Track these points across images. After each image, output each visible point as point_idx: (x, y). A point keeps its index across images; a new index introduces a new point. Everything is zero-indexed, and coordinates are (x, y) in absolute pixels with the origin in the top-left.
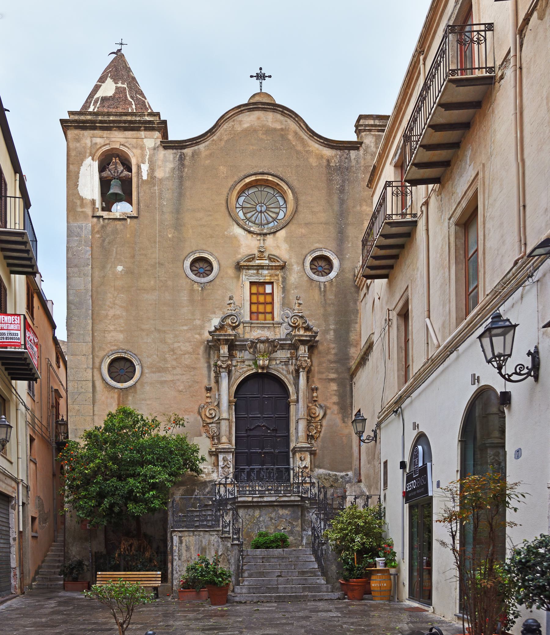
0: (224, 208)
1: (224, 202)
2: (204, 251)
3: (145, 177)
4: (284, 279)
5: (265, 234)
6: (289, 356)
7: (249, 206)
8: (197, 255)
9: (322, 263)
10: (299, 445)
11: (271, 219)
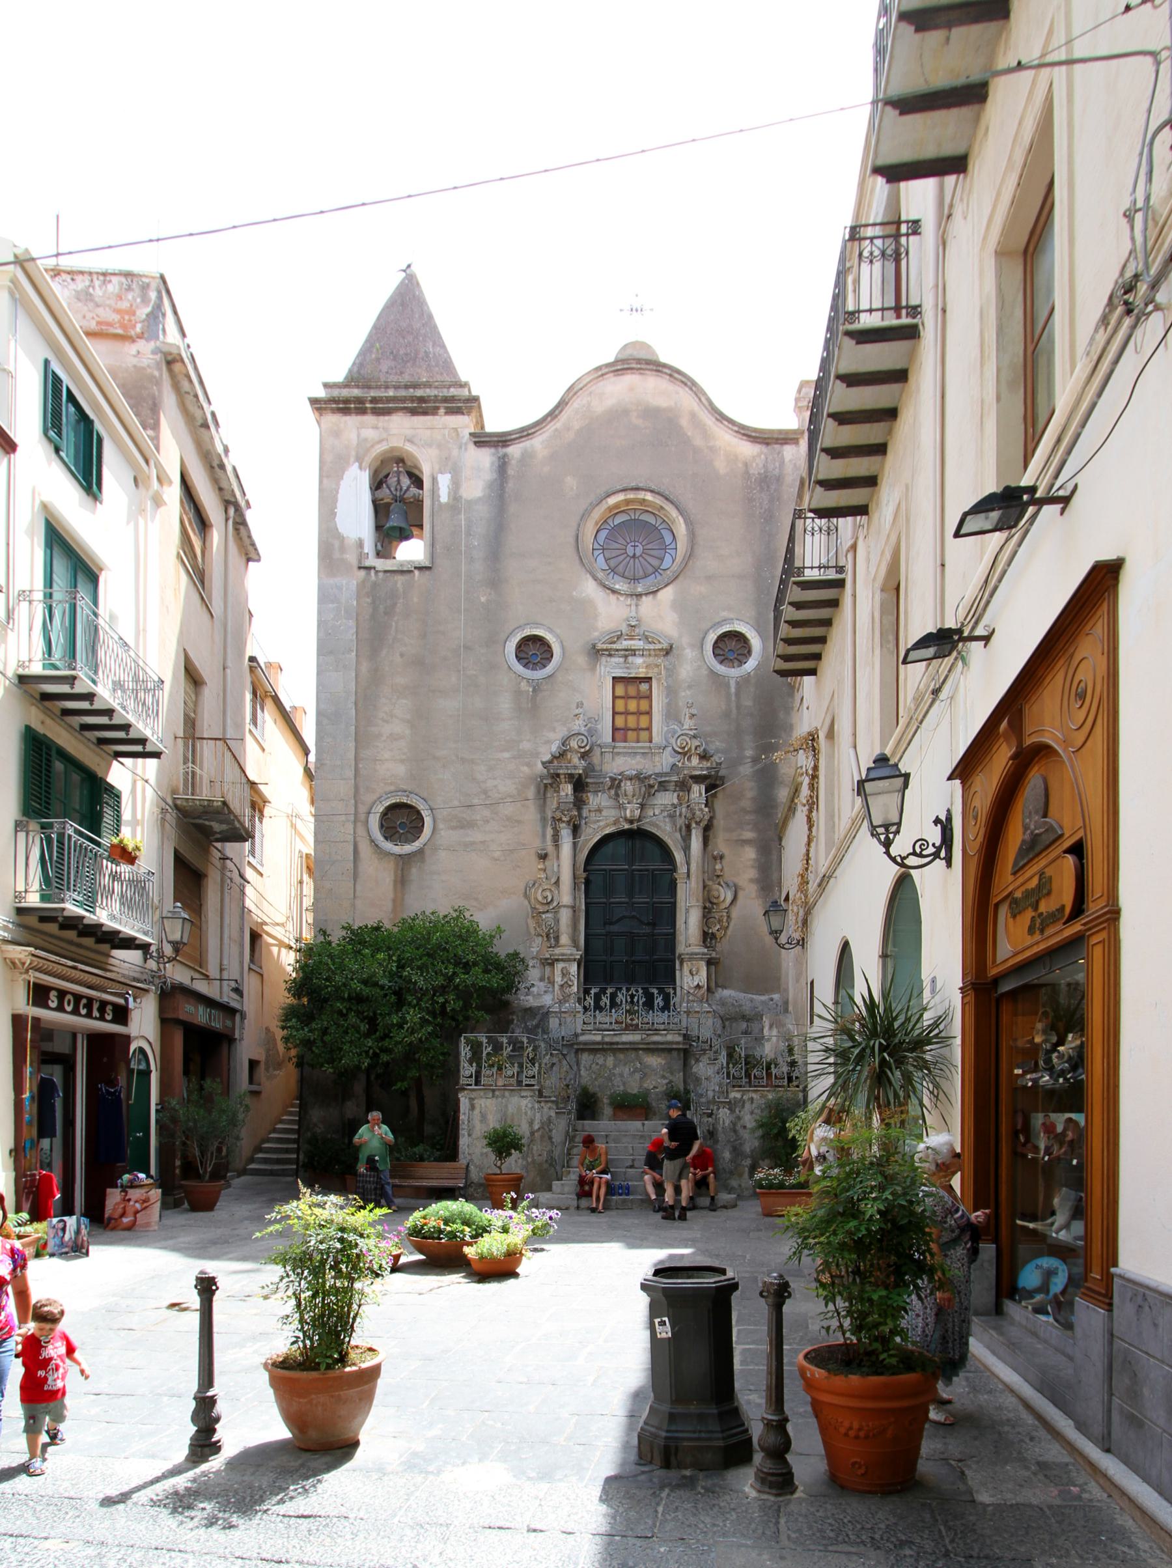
0: (570, 550)
1: (572, 540)
2: (538, 625)
3: (444, 497)
4: (671, 672)
5: (639, 596)
6: (676, 801)
8: (528, 632)
9: (732, 644)
10: (689, 950)
11: (651, 570)
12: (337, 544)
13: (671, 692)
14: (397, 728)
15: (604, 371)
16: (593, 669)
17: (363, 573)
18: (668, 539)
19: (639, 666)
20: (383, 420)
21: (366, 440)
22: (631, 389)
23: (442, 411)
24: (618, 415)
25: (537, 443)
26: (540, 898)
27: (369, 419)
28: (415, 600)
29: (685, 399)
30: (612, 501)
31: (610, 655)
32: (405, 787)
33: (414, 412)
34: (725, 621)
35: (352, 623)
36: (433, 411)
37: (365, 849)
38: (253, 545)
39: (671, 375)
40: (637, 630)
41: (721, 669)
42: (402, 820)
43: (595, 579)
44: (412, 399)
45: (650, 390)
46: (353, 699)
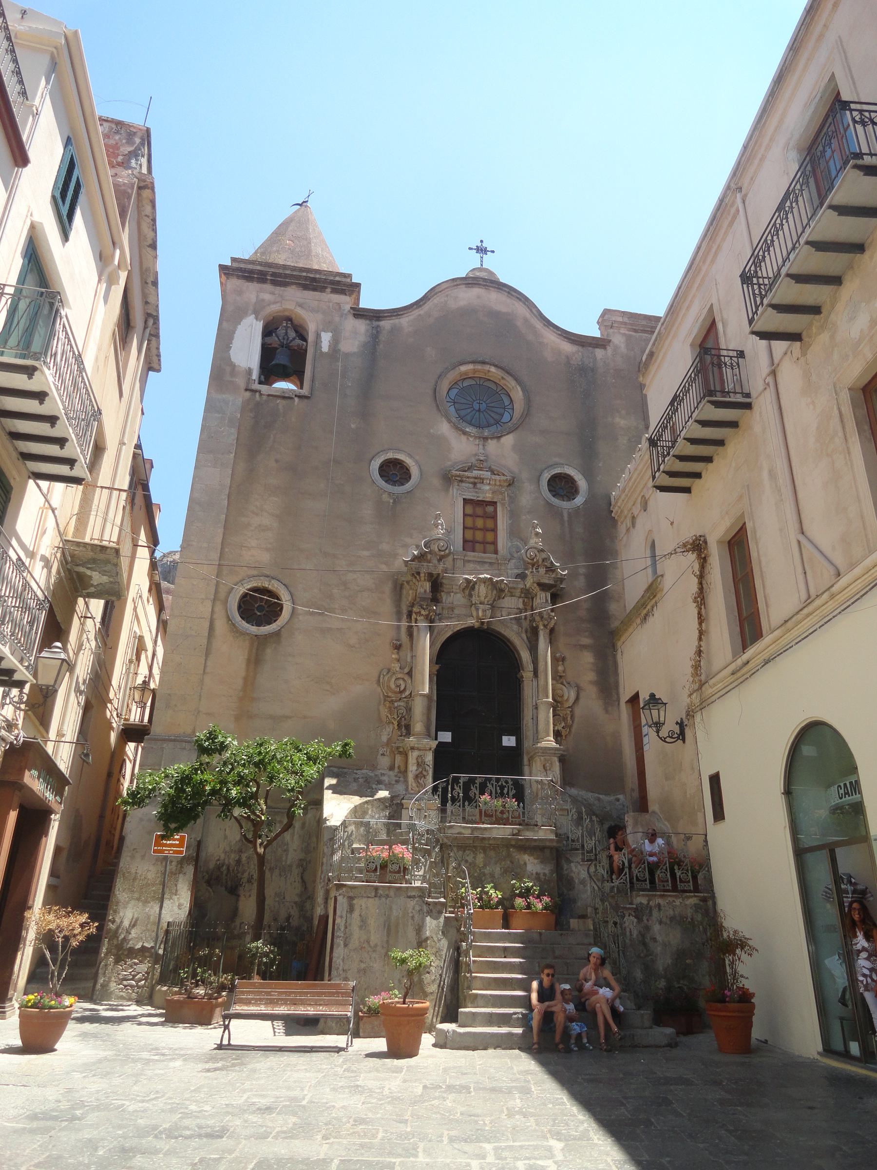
2: (399, 450)
3: (325, 348)
4: (513, 500)
5: (485, 439)
6: (521, 606)
7: (465, 401)
8: (390, 455)
11: (492, 421)
12: (228, 369)
13: (514, 515)
14: (266, 520)
15: (458, 282)
16: (447, 490)
17: (248, 394)
18: (507, 402)
19: (486, 493)
20: (278, 290)
21: (263, 300)
22: (478, 297)
23: (329, 290)
24: (467, 312)
25: (404, 321)
26: (393, 686)
27: (268, 287)
28: (293, 420)
29: (521, 310)
30: (463, 368)
31: (461, 481)
32: (268, 573)
33: (305, 287)
34: (557, 464)
35: (234, 431)
36: (322, 289)
37: (221, 626)
38: (159, 356)
39: (509, 293)
40: (485, 464)
41: (555, 501)
42: (259, 606)
43: (449, 421)
44: (306, 278)
45: (494, 299)
46: (227, 492)
